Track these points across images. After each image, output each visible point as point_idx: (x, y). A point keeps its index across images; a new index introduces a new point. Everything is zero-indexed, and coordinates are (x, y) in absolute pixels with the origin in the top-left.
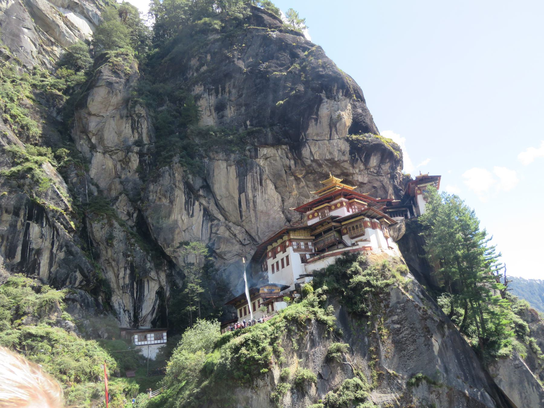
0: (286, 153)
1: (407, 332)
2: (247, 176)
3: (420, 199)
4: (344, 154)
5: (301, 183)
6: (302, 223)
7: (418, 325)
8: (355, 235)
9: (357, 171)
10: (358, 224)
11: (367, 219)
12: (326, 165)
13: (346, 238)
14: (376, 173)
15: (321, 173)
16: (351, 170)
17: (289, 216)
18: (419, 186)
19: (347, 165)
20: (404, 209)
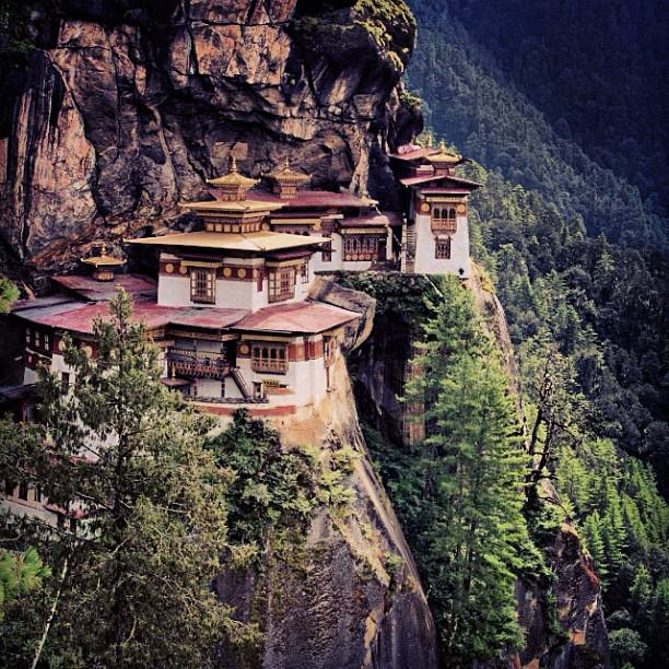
0: (131, 47)
1: (325, 603)
2: (21, 97)
3: (423, 222)
4: (272, 68)
5: (152, 123)
6: (133, 218)
7: (348, 592)
8: (265, 369)
9: (295, 111)
10: (278, 348)
11: (299, 341)
12: (224, 88)
13: (244, 366)
14: (341, 115)
15: (207, 103)
16: (282, 109)
17: (107, 202)
18: (428, 199)
19: (272, 97)
20: (381, 231)
